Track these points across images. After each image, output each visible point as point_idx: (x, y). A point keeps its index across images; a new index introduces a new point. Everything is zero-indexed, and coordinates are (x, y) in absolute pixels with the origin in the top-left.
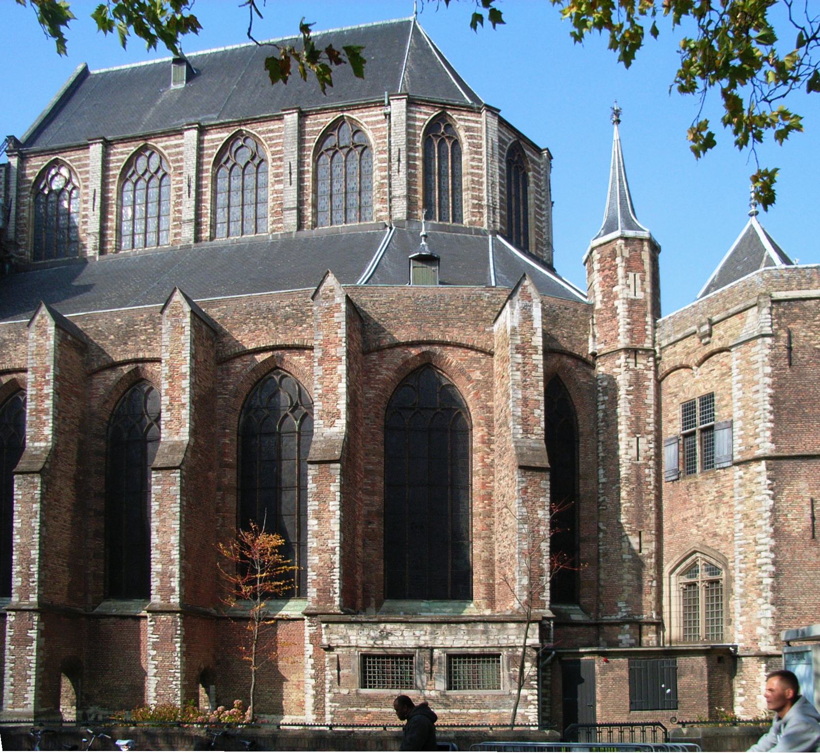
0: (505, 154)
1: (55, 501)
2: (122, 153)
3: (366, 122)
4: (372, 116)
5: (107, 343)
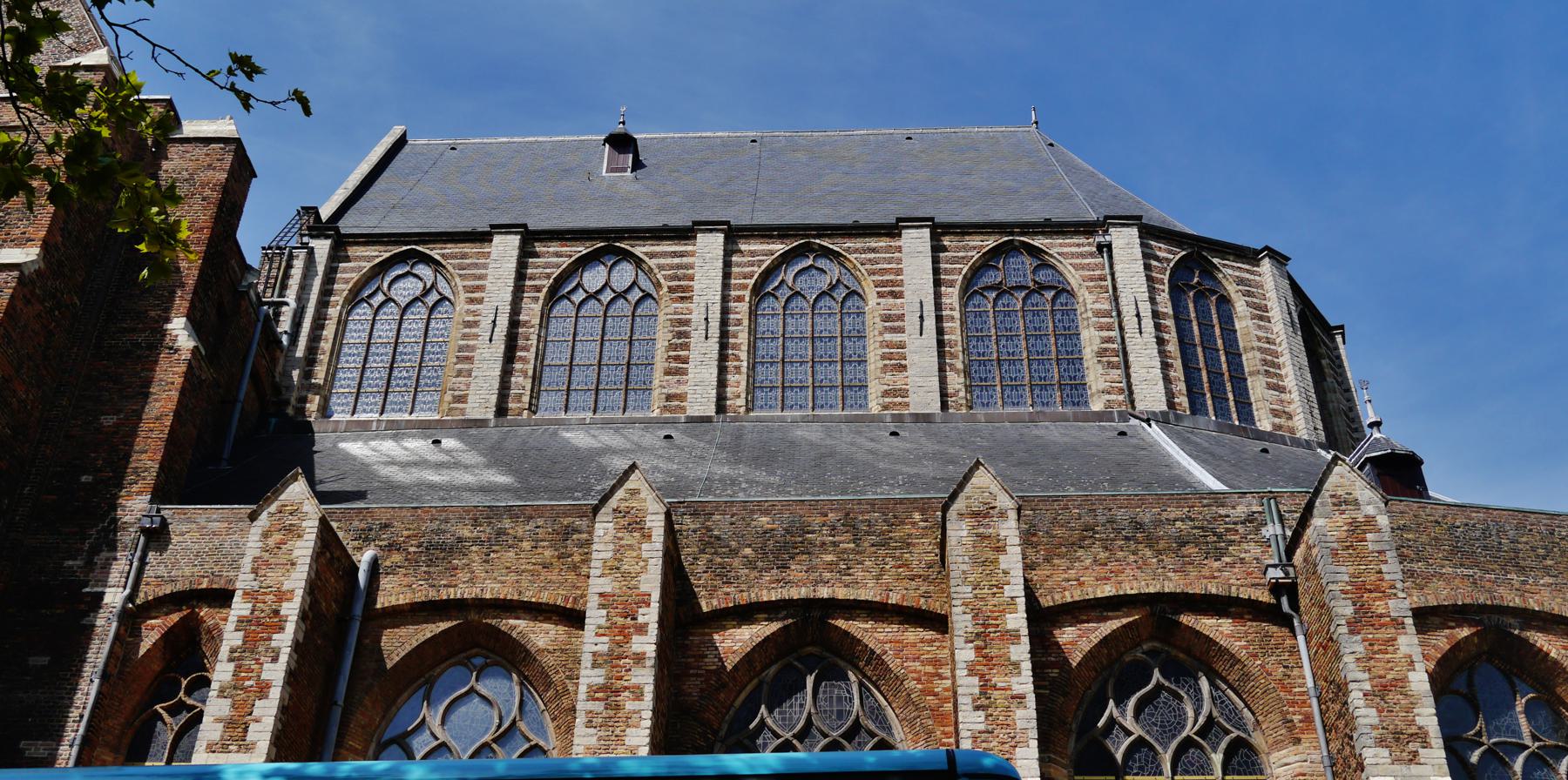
2: (558, 255)
3: (1058, 253)
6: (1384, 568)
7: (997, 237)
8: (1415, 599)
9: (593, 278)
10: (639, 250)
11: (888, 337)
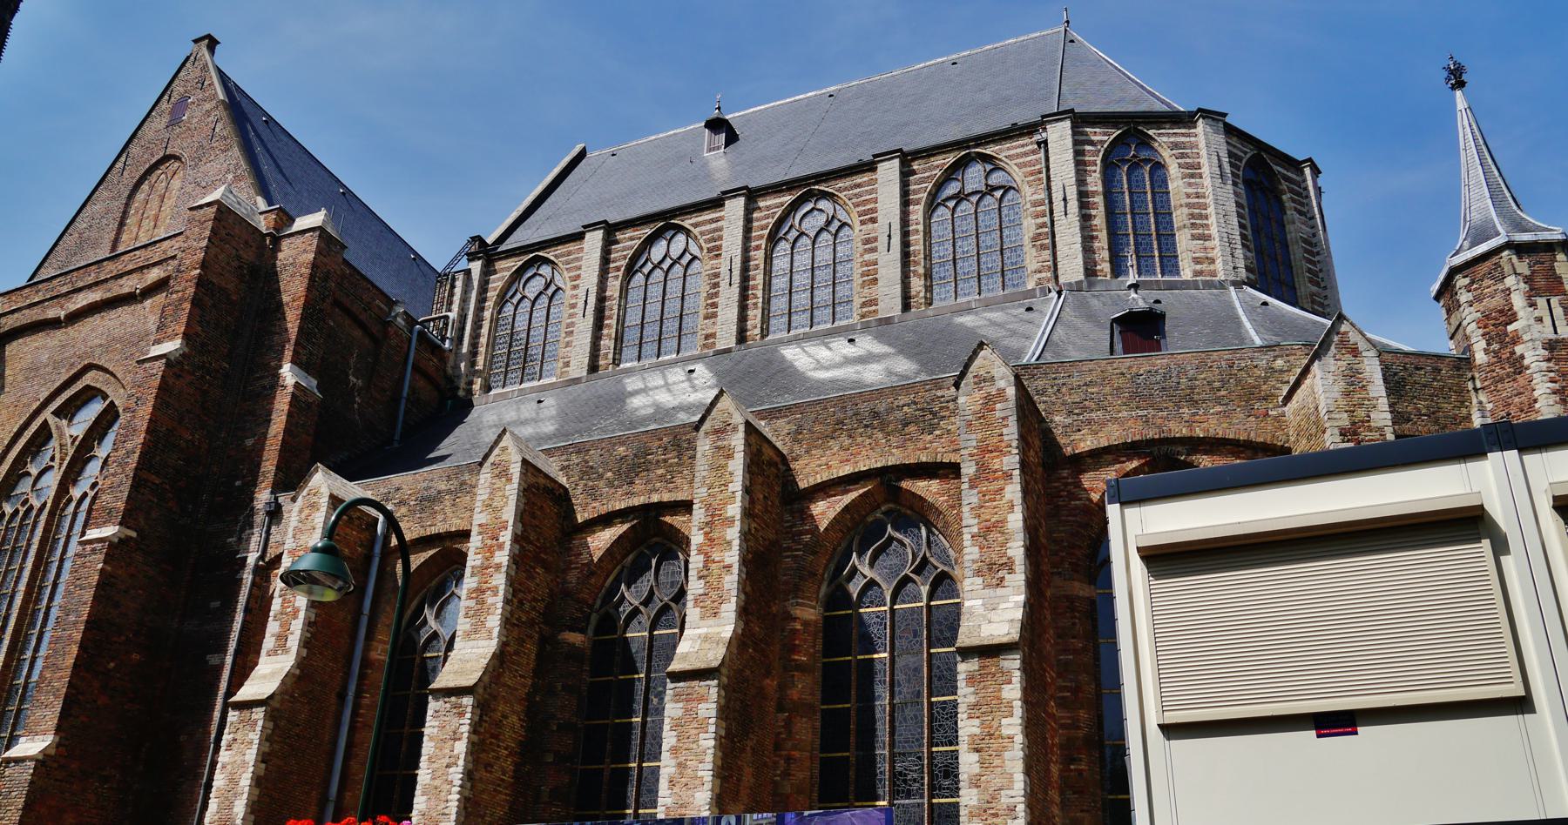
0: (1241, 173)
1: (494, 736)
2: (631, 239)
3: (1006, 157)
4: (1016, 147)
5: (601, 484)
6: (1005, 431)
7: (956, 153)
8: (1088, 443)
9: (657, 252)
10: (687, 224)
11: (867, 257)
